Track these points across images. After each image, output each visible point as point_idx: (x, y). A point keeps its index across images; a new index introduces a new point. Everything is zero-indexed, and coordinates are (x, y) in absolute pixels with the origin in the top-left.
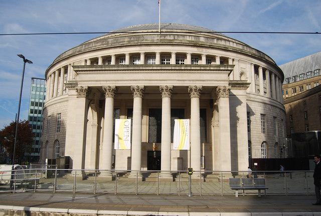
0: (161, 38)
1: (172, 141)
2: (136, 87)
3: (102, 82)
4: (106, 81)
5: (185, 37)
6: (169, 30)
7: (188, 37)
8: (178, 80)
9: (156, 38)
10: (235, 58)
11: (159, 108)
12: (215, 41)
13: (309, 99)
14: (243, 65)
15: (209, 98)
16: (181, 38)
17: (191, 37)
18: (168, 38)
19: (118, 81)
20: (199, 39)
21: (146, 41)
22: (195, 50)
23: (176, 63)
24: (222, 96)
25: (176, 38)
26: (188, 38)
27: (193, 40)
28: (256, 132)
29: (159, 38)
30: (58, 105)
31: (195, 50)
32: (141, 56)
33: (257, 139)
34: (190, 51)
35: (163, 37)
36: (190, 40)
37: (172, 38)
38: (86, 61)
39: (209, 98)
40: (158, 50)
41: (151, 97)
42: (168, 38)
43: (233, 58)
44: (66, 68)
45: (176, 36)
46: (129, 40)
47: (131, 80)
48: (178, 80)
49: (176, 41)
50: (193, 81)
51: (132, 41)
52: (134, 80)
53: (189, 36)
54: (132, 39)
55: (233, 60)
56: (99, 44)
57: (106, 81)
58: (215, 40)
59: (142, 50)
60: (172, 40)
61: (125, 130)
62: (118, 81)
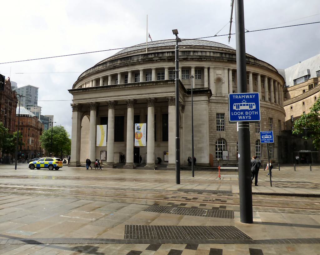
0: (145, 58)
2: (109, 102)
6: (155, 49)
10: (210, 66)
12: (192, 54)
14: (219, 72)
15: (161, 106)
16: (161, 55)
17: (169, 53)
18: (150, 56)
22: (171, 65)
24: (170, 104)
25: (156, 55)
28: (231, 131)
29: (142, 58)
32: (129, 74)
33: (233, 137)
35: (146, 57)
36: (169, 55)
39: (161, 106)
40: (141, 68)
41: (120, 107)
42: (150, 56)
43: (208, 66)
50: (148, 94)
53: (168, 52)
55: (209, 69)
58: (192, 54)
60: (153, 58)
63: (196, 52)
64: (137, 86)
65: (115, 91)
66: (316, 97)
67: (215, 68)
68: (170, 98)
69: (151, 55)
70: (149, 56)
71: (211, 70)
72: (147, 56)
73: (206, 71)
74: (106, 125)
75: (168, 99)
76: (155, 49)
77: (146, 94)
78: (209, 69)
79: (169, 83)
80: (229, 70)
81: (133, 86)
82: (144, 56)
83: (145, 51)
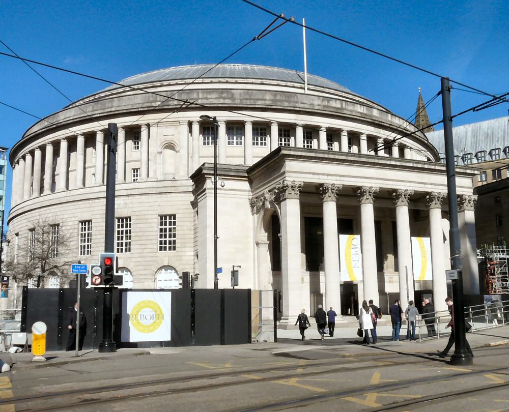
1: (340, 271)
3: (321, 177)
4: (328, 175)
6: (318, 88)
7: (334, 101)
8: (418, 183)
9: (317, 104)
11: (319, 216)
16: (350, 107)
17: (362, 107)
19: (343, 176)
20: (372, 112)
21: (302, 106)
23: (329, 149)
24: (467, 208)
25: (344, 106)
27: (365, 112)
34: (367, 130)
36: (362, 111)
38: (190, 124)
40: (325, 123)
41: (386, 200)
44: (133, 133)
45: (344, 103)
47: (360, 177)
48: (418, 183)
49: (345, 112)
50: (435, 185)
51: (279, 101)
52: (364, 178)
54: (278, 97)
56: (214, 96)
57: (328, 175)
59: (325, 123)
61: (353, 251)
62: (343, 176)
63: (394, 117)
68: (467, 197)
69: (336, 101)
70: (331, 102)
72: (328, 102)
74: (358, 237)
76: (318, 88)
77: (431, 184)
82: (323, 100)
83: (304, 89)
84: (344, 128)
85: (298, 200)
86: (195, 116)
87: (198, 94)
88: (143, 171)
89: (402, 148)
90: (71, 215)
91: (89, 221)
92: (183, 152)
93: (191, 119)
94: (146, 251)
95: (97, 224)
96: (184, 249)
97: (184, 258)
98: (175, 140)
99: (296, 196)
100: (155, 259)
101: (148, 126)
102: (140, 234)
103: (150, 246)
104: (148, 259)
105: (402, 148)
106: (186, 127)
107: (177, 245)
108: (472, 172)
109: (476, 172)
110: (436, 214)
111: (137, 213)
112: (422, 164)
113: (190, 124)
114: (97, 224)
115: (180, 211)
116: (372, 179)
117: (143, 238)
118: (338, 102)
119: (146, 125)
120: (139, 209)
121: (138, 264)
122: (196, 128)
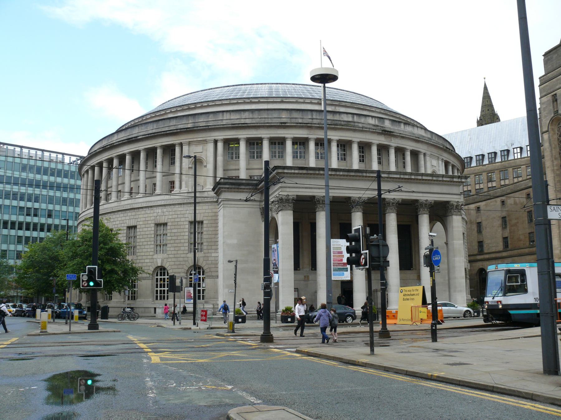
5: (367, 118)
13: (486, 205)
14: (435, 162)
17: (374, 119)
20: (384, 122)
22: (383, 140)
24: (454, 213)
26: (371, 121)
30: (159, 210)
31: (383, 140)
34: (376, 140)
37: (350, 118)
38: (216, 142)
42: (345, 118)
44: (169, 150)
46: (289, 116)
53: (372, 117)
55: (425, 154)
64: (407, 177)
65: (359, 180)
66: (478, 208)
67: (432, 156)
71: (428, 158)
73: (421, 157)
75: (453, 205)
78: (425, 154)
79: (455, 180)
80: (442, 159)
81: (402, 176)
84: (354, 140)
85: (291, 212)
86: (221, 135)
87: (223, 115)
88: (177, 184)
89: (415, 154)
90: (121, 222)
91: (135, 227)
92: (210, 166)
93: (216, 138)
94: (179, 252)
95: (141, 230)
96: (210, 251)
97: (210, 259)
98: (203, 156)
99: (289, 208)
100: (186, 259)
101: (181, 145)
102: (174, 238)
103: (182, 248)
104: (181, 259)
105: (415, 154)
106: (211, 146)
107: (205, 247)
108: (460, 180)
109: (463, 180)
110: (424, 220)
111: (172, 220)
112: (409, 175)
113: (216, 142)
114: (141, 230)
115: (205, 218)
116: (363, 191)
117: (177, 241)
118: (350, 116)
119: (179, 144)
120: (174, 216)
121: (173, 263)
122: (220, 145)
